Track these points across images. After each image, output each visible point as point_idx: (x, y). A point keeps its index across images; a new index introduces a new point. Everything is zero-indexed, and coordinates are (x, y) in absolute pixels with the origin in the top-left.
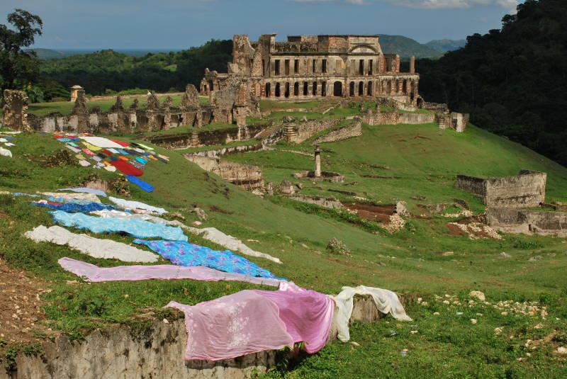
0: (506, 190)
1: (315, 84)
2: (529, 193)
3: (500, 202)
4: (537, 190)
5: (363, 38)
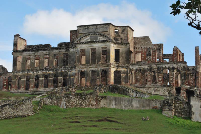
5: (95, 27)
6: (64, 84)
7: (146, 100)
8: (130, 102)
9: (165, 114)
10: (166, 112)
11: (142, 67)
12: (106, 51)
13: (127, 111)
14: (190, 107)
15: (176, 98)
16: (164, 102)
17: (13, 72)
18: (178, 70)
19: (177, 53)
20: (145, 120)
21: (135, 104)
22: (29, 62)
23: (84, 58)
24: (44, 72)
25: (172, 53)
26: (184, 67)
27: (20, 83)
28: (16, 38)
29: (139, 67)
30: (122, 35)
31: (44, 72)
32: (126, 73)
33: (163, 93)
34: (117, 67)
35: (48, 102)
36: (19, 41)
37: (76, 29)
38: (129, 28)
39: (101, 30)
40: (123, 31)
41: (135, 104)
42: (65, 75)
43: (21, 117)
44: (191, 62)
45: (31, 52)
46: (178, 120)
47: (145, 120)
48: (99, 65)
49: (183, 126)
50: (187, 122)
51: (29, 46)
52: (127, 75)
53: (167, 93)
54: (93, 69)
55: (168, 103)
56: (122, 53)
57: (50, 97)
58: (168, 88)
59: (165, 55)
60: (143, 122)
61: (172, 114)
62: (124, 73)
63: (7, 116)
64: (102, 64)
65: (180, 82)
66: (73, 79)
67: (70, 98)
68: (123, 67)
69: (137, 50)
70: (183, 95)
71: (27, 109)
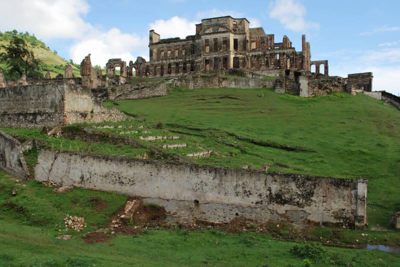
0: (12, 103)
1: (185, 64)
2: (42, 109)
3: (6, 118)
4: (51, 107)
5: (217, 20)
6: (192, 70)
7: (261, 80)
8: (247, 82)
9: (277, 91)
10: (278, 90)
11: (257, 53)
12: (226, 41)
13: (245, 89)
14: (299, 85)
15: (287, 78)
16: (276, 81)
17: (150, 62)
18: (288, 56)
19: (287, 41)
20: (261, 96)
21: (252, 84)
22: (163, 53)
23: (208, 48)
24: (175, 61)
25: (282, 42)
26: (293, 52)
27: (156, 70)
28: (151, 33)
29: (254, 54)
30: (240, 27)
31: (175, 61)
32: (244, 59)
33: (274, 74)
34: (236, 53)
35: (178, 84)
36: (154, 36)
37: (201, 22)
38: (245, 21)
39: (222, 22)
40: (241, 23)
41: (252, 84)
42: (192, 62)
43: (157, 96)
44: (299, 49)
45: (164, 45)
46: (289, 95)
47: (261, 96)
48: (220, 53)
49: (292, 101)
50: (296, 97)
51: (163, 40)
52: (244, 60)
53: (278, 75)
54: (215, 56)
55: (280, 82)
56: (240, 42)
57: (180, 80)
58: (279, 71)
59: (276, 44)
60: (259, 98)
61: (283, 91)
62: (242, 59)
63: (146, 96)
64: (223, 52)
65: (288, 66)
66: (199, 65)
67: (197, 80)
68: (240, 54)
69: (252, 40)
70: (292, 76)
71: (161, 90)
